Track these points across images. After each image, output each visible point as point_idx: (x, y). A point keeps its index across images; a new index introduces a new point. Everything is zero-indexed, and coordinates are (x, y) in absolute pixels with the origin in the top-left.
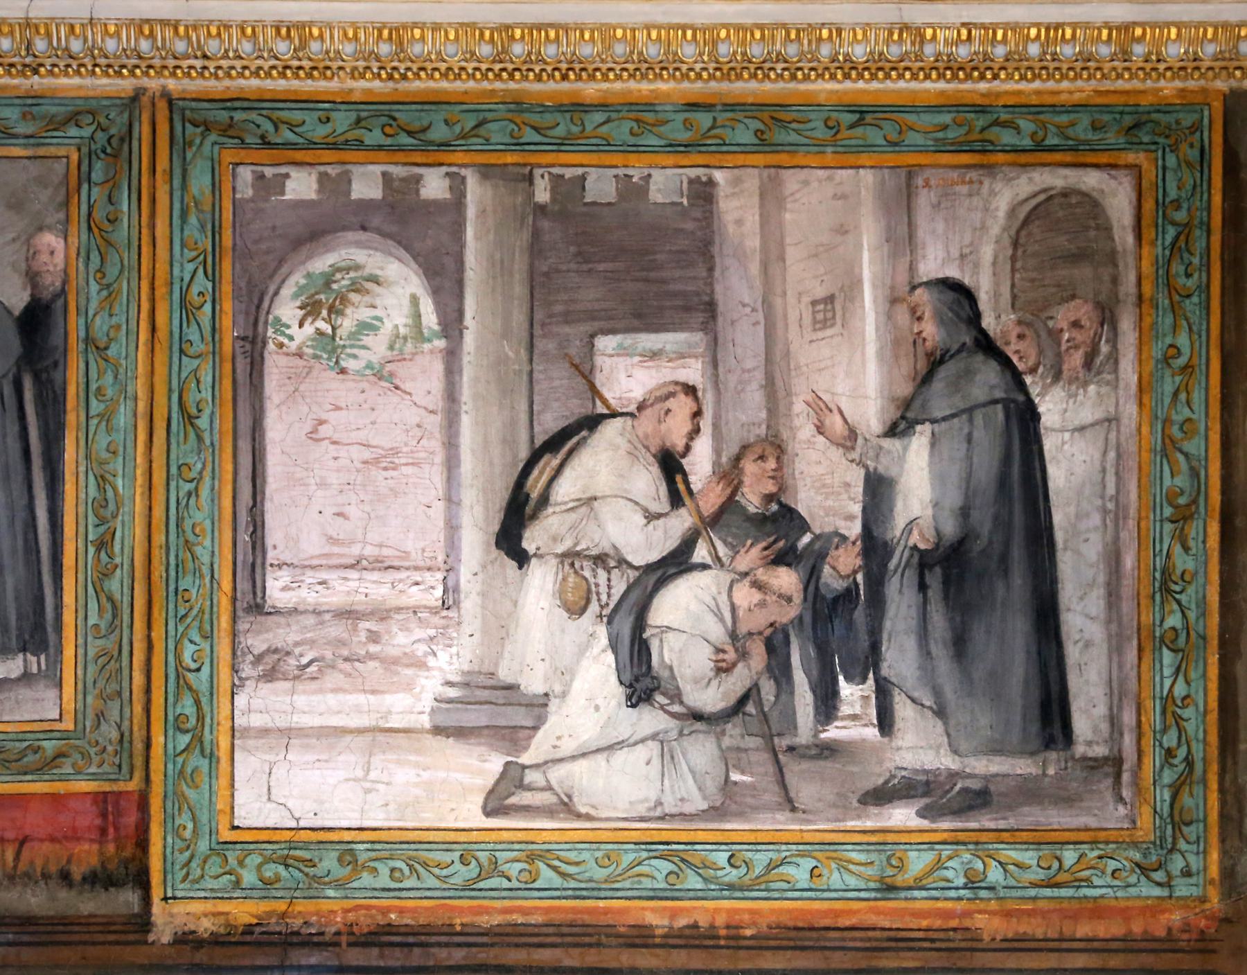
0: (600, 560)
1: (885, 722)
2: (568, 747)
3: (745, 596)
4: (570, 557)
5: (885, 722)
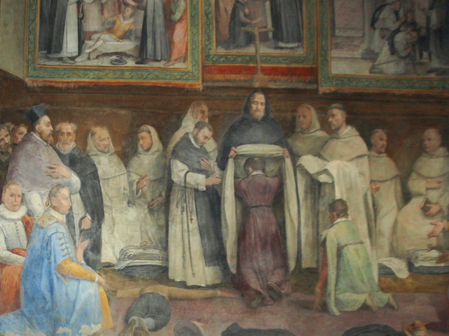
0: (386, 29)
1: (430, 59)
2: (382, 62)
3: (408, 36)
4: (382, 29)
5: (430, 59)
